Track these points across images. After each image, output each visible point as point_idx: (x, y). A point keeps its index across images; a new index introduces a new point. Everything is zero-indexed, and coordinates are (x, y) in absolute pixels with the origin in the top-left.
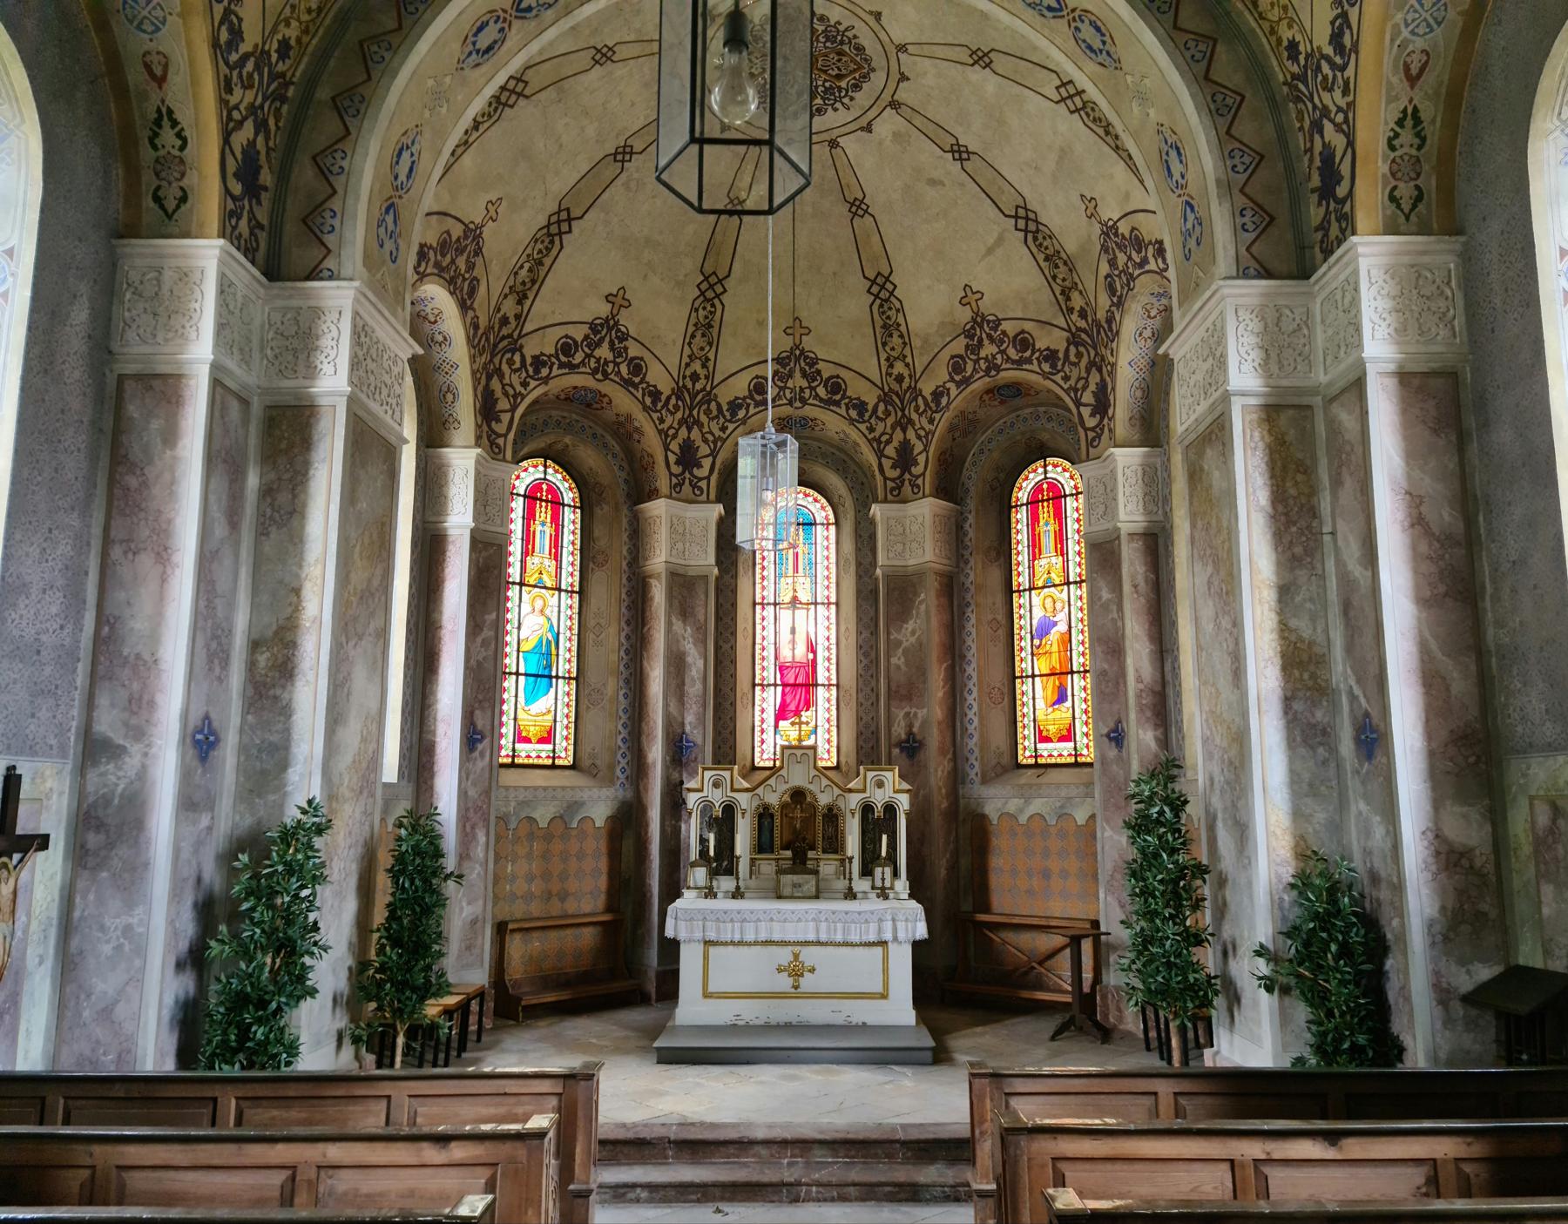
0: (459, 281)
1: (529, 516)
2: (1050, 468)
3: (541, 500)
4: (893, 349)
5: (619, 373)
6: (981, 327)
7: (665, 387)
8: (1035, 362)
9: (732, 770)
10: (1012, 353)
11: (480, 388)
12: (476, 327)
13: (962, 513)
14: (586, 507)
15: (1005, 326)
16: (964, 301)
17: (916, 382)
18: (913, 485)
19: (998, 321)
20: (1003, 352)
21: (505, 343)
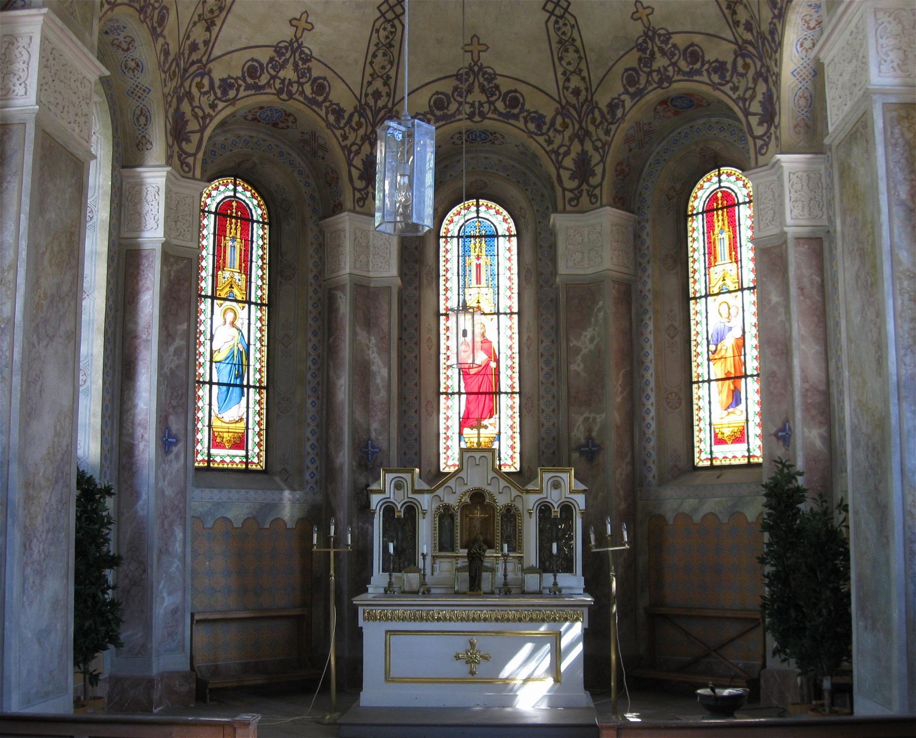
0: (149, 11)
1: (220, 232)
2: (724, 177)
3: (231, 217)
4: (569, 63)
5: (302, 93)
6: (653, 40)
7: (348, 104)
8: (705, 73)
9: (412, 472)
10: (683, 64)
11: (171, 110)
12: (167, 53)
13: (639, 223)
14: (273, 222)
15: (676, 39)
16: (635, 16)
17: (592, 95)
18: (591, 195)
19: (668, 36)
20: (674, 64)
21: (195, 67)
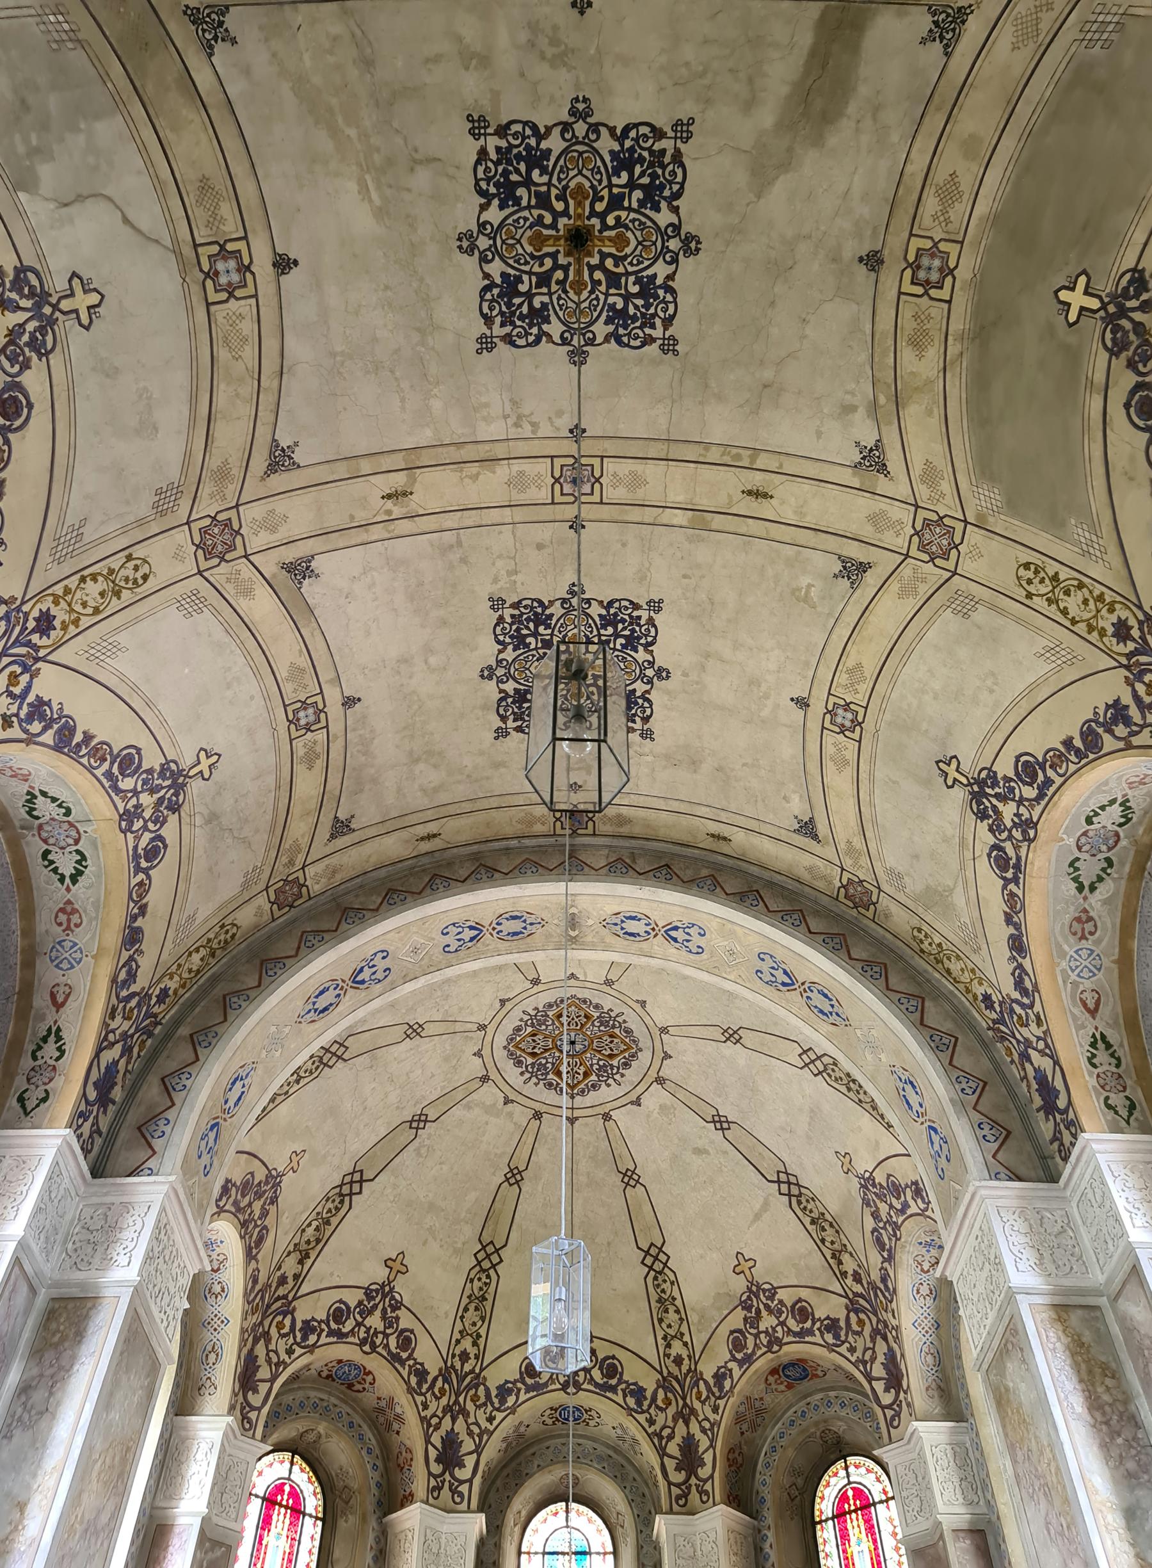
0: (251, 1227)
1: (266, 1522)
3: (281, 1505)
4: (669, 1326)
5: (387, 1346)
6: (757, 1297)
7: (433, 1366)
8: (817, 1332)
10: (792, 1323)
11: (245, 1351)
12: (255, 1281)
13: (759, 1531)
14: (329, 1519)
15: (781, 1294)
16: (737, 1270)
17: (696, 1364)
18: (702, 1492)
19: (773, 1292)
20: (783, 1324)
21: (279, 1304)
